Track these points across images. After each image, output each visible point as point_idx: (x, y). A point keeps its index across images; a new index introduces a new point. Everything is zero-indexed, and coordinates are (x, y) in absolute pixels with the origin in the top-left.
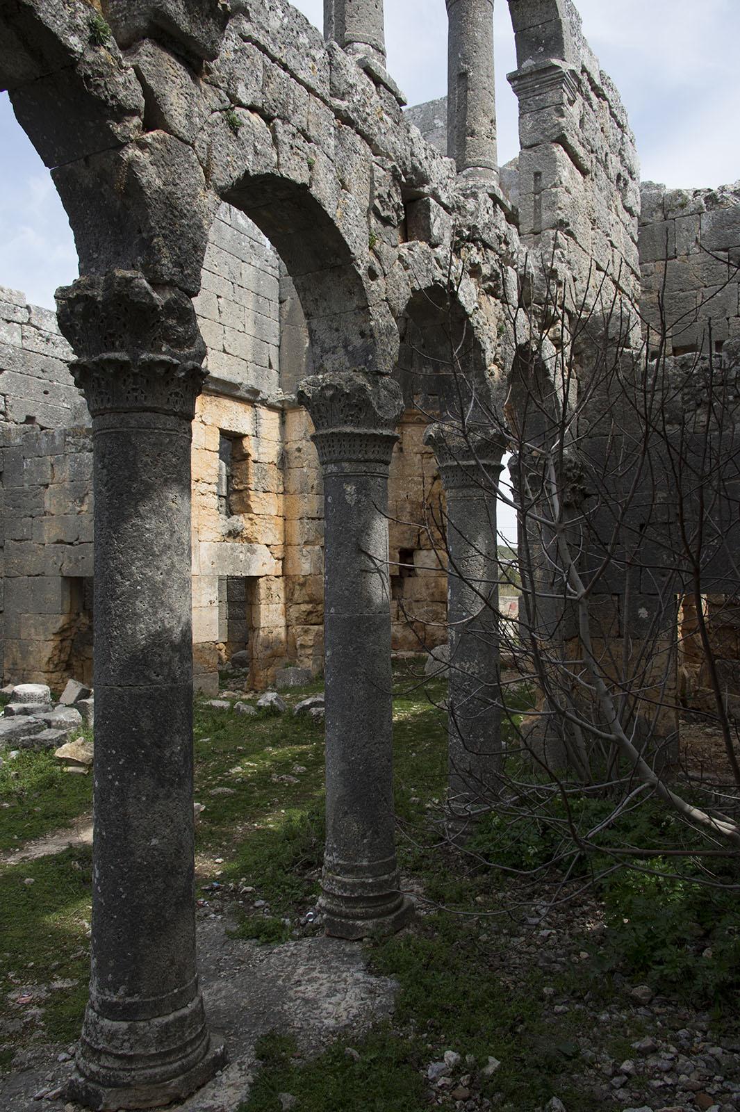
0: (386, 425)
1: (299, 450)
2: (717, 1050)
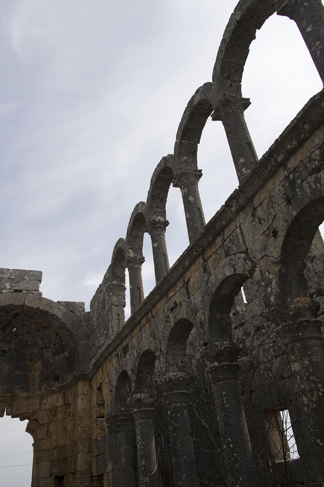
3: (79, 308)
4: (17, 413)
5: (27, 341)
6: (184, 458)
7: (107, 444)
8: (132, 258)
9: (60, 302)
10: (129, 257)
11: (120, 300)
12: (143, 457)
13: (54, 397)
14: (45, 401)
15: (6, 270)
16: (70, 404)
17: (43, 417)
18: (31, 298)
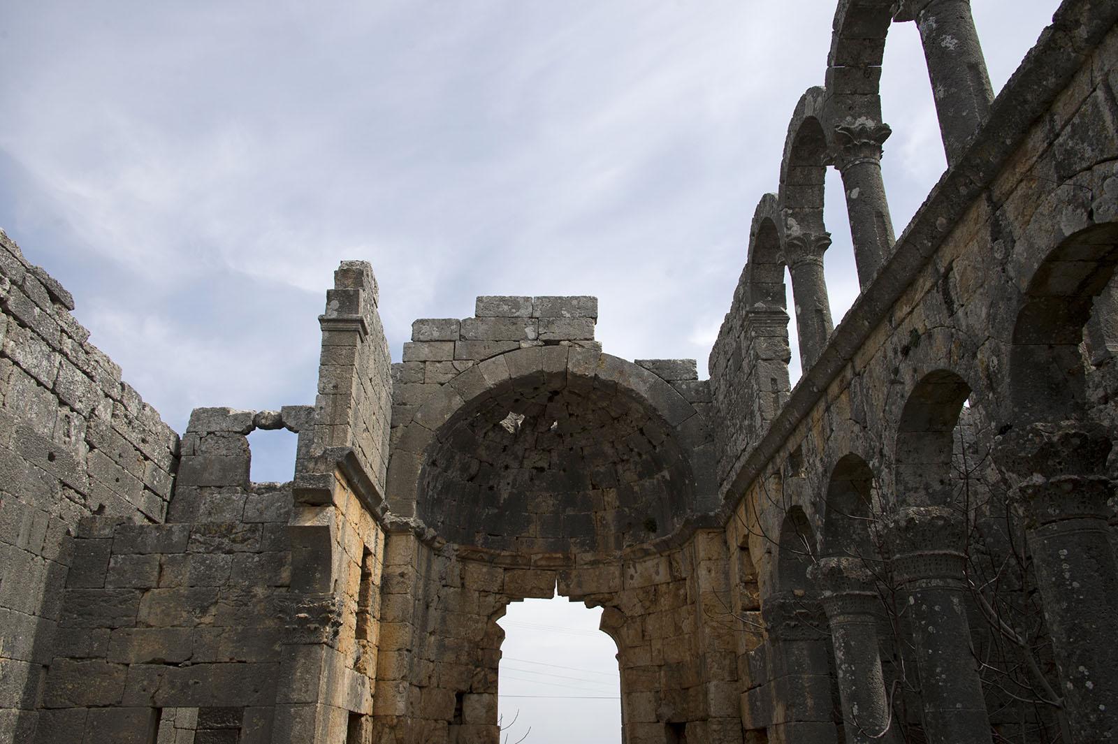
1: (402, 575)
3: (684, 373)
4: (578, 592)
5: (582, 448)
6: (957, 706)
7: (770, 666)
8: (797, 238)
9: (640, 361)
10: (788, 236)
11: (776, 345)
12: (853, 698)
13: (650, 563)
14: (632, 571)
15: (523, 300)
16: (685, 579)
17: (632, 604)
18: (579, 357)
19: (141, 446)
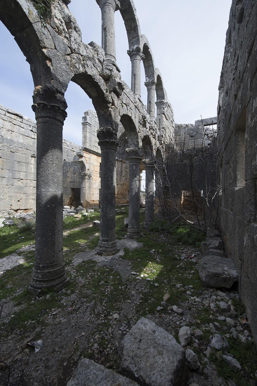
0: (140, 157)
2: (193, 249)
19: (72, 149)
